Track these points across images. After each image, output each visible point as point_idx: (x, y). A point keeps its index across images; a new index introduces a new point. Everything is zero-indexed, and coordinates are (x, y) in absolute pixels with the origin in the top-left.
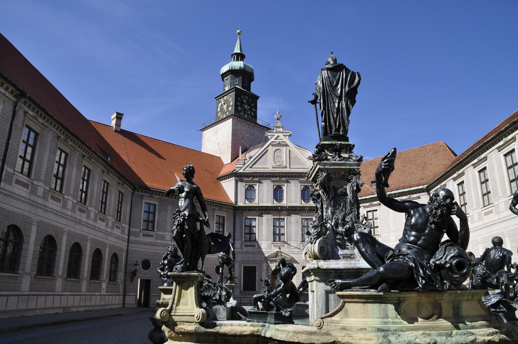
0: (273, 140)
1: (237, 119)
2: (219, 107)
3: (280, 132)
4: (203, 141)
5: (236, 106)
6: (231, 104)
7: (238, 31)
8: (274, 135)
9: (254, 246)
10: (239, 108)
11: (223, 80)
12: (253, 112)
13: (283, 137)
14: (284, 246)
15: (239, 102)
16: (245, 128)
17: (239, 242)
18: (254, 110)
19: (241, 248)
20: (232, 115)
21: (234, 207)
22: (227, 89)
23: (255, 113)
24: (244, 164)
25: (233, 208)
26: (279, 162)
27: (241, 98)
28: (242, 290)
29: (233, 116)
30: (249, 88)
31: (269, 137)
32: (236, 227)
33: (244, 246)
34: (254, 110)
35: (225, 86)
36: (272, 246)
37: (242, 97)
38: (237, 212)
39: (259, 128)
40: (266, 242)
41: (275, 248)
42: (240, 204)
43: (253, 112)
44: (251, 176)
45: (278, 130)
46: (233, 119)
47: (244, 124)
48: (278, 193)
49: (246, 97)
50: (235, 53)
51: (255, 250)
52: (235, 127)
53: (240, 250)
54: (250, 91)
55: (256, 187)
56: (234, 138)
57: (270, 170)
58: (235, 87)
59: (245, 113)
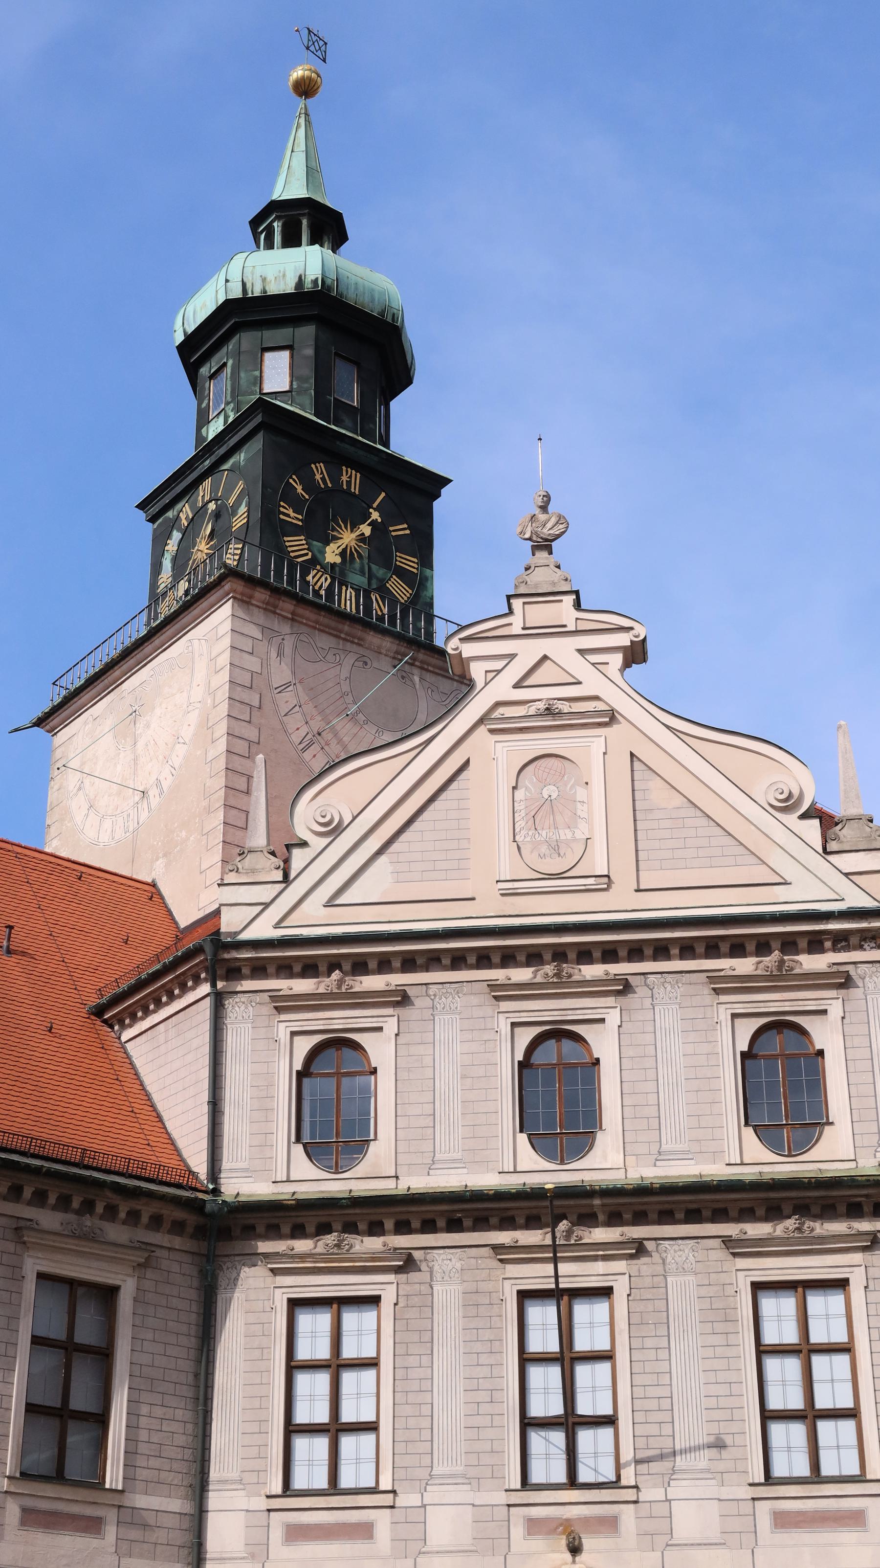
0: (501, 688)
1: (270, 609)
2: (167, 564)
3: (559, 631)
4: (53, 796)
5: (270, 530)
6: (239, 521)
7: (298, 73)
8: (512, 656)
9: (365, 1531)
10: (296, 545)
12: (401, 573)
13: (580, 667)
14: (611, 1524)
15: (297, 504)
17: (240, 1500)
20: (231, 573)
21: (197, 1206)
22: (215, 428)
23: (420, 584)
25: (191, 1219)
26: (556, 849)
27: (309, 484)
29: (239, 586)
31: (477, 671)
33: (277, 1534)
34: (409, 563)
35: (203, 419)
36: (518, 1531)
37: (320, 472)
40: (463, 1494)
41: (538, 1544)
42: (243, 1183)
43: (401, 573)
44: (334, 964)
45: (541, 614)
47: (325, 641)
48: (556, 1090)
49: (351, 480)
50: (275, 207)
52: (253, 664)
57: (489, 909)
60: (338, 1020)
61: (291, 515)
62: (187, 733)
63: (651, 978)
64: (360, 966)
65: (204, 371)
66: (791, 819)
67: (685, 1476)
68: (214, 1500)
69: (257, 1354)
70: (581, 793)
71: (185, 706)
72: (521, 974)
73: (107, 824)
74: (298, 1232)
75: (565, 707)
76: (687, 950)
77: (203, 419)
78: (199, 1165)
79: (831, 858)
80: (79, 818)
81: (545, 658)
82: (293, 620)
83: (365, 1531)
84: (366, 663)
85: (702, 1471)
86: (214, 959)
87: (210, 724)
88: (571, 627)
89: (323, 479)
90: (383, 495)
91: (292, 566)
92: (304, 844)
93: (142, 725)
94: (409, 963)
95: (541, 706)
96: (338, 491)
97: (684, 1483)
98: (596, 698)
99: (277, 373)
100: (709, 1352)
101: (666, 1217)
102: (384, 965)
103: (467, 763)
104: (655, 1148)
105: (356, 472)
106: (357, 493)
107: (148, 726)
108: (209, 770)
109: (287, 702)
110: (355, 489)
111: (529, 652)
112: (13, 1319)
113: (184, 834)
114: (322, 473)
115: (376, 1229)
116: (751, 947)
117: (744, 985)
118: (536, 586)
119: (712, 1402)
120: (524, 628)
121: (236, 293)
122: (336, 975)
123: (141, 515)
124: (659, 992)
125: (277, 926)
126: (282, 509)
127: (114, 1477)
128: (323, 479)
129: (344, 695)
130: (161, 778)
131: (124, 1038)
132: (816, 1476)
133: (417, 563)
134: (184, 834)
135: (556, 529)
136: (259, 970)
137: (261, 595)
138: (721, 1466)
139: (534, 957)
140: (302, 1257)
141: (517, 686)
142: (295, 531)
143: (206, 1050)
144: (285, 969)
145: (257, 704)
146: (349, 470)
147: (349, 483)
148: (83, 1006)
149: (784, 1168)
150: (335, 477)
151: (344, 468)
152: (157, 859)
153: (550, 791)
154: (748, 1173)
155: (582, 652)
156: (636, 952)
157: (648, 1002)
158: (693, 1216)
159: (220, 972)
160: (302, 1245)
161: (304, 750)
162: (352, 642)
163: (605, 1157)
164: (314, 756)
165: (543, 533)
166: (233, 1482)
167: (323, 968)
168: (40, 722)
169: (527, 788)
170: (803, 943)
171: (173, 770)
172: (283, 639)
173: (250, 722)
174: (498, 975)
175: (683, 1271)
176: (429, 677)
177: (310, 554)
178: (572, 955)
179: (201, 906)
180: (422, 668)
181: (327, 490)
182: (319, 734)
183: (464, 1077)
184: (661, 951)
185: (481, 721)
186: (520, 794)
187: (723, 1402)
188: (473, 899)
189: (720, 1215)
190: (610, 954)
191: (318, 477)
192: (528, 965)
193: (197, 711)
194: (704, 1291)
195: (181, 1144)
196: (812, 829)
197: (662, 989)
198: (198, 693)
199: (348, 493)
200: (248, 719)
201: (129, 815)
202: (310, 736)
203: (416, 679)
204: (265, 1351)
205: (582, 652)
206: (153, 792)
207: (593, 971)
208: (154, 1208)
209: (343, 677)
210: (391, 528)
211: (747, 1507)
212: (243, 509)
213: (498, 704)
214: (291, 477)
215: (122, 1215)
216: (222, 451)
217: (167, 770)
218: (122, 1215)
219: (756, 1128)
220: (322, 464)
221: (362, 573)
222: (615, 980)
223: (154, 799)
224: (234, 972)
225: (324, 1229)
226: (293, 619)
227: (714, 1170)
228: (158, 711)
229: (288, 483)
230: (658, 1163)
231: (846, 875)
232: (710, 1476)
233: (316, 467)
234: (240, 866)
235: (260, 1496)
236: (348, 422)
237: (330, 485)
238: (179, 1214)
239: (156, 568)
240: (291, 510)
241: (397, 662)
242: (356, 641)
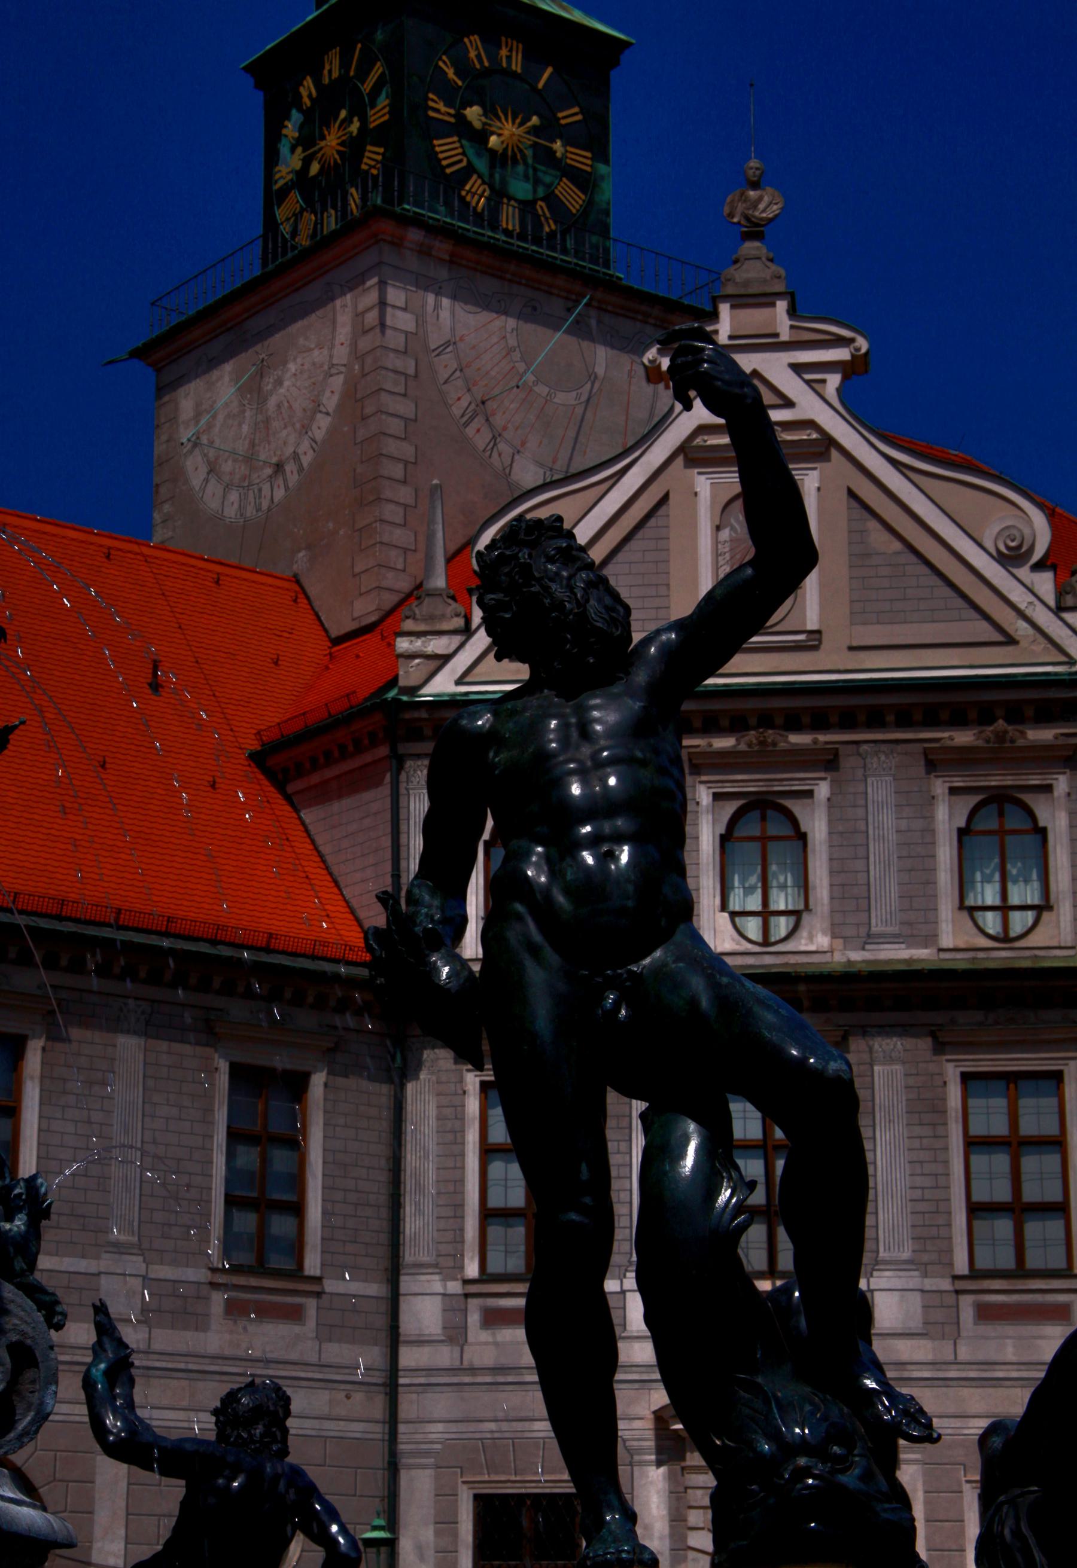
17: (436, 1284)
19: (455, 1334)
27: (463, 68)
32: (411, 1160)
33: (474, 1318)
37: (474, 48)
53: (445, 1356)
62: (331, 402)
63: (864, 747)
67: (888, 1267)
68: (407, 1284)
69: (449, 1137)
71: (326, 367)
73: (234, 496)
76: (904, 720)
80: (196, 482)
82: (451, 262)
84: (535, 309)
85: (906, 1262)
87: (359, 396)
88: (785, 337)
89: (479, 56)
90: (550, 70)
93: (271, 380)
96: (496, 71)
97: (887, 1273)
100: (916, 1143)
103: (665, 499)
104: (863, 931)
105: (518, 42)
106: (519, 71)
107: (279, 382)
108: (359, 452)
109: (446, 366)
110: (517, 66)
112: (209, 1110)
113: (331, 525)
114: (477, 48)
118: (747, 283)
119: (918, 1194)
124: (873, 762)
125: (459, 682)
126: (431, 104)
127: (312, 1264)
128: (479, 56)
129: (510, 351)
130: (300, 451)
132: (1021, 1271)
133: (592, 159)
134: (331, 525)
135: (769, 211)
138: (925, 1258)
145: (411, 371)
146: (509, 40)
147: (509, 58)
148: (240, 751)
149: (1002, 957)
150: (494, 58)
151: (503, 39)
152: (299, 551)
157: (860, 773)
161: (466, 424)
162: (519, 283)
163: (811, 938)
164: (478, 431)
165: (754, 217)
166: (429, 1266)
168: (137, 354)
169: (733, 529)
171: (314, 445)
172: (440, 288)
173: (405, 395)
175: (890, 1060)
177: (465, 160)
179: (356, 615)
180: (599, 309)
181: (486, 73)
182: (483, 403)
186: (725, 534)
187: (928, 1194)
191: (472, 54)
193: (341, 377)
194: (911, 1081)
197: (875, 759)
198: (341, 353)
200: (403, 391)
201: (260, 490)
202: (473, 406)
203: (593, 322)
204: (458, 1135)
206: (290, 467)
209: (509, 329)
210: (560, 115)
211: (951, 1299)
212: (383, 101)
214: (440, 59)
215: (310, 1000)
217: (305, 445)
218: (310, 1000)
220: (476, 37)
221: (526, 178)
223: (292, 476)
226: (453, 262)
227: (922, 954)
228: (292, 367)
229: (437, 66)
230: (867, 947)
232: (914, 1267)
233: (471, 42)
234: (417, 612)
235: (457, 1280)
237: (486, 64)
239: (272, 157)
240: (442, 104)
241: (570, 304)
242: (523, 281)
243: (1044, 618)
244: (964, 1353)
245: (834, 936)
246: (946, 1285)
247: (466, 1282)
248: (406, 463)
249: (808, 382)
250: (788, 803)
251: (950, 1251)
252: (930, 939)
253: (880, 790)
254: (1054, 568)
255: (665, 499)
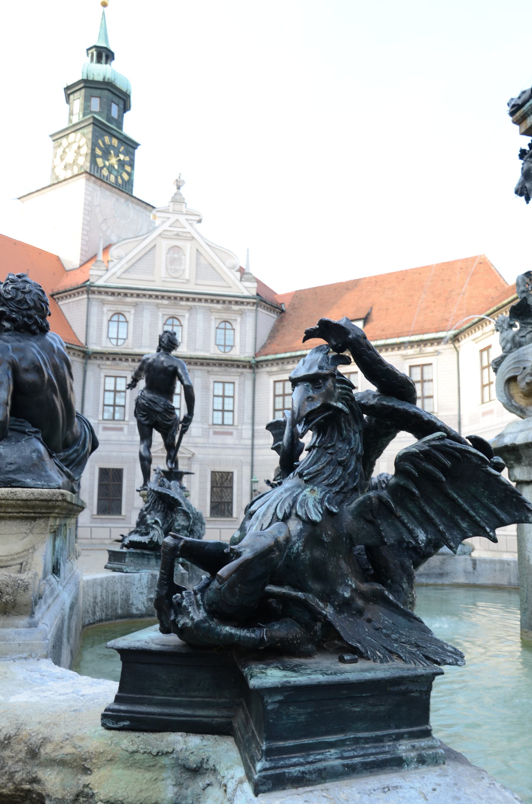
0: (166, 226)
1: (95, 183)
5: (94, 156)
8: (169, 218)
9: (121, 429)
10: (100, 161)
11: (68, 101)
13: (186, 224)
16: (109, 201)
18: (128, 168)
24: (107, 270)
25: (82, 354)
26: (176, 271)
28: (95, 512)
29: (88, 175)
30: (119, 123)
32: (87, 392)
37: (107, 139)
38: (89, 362)
39: (138, 204)
44: (119, 294)
46: (88, 180)
47: (108, 193)
49: (115, 142)
51: (123, 438)
54: (121, 128)
55: (130, 317)
56: (88, 218)
58: (94, 118)
59: (110, 173)
60: (120, 308)
61: (98, 152)
64: (126, 295)
65: (71, 97)
66: (233, 271)
70: (183, 257)
72: (165, 302)
74: (108, 359)
75: (181, 234)
77: (71, 114)
78: (83, 341)
79: (243, 283)
81: (177, 220)
83: (121, 429)
86: (87, 288)
91: (98, 167)
92: (112, 261)
94: (138, 296)
95: (176, 233)
98: (189, 233)
99: (95, 104)
101: (196, 364)
102: (132, 295)
103: (155, 246)
110: (116, 145)
111: (173, 218)
115: (127, 360)
116: (221, 302)
117: (219, 311)
120: (173, 211)
121: (85, 78)
122: (120, 297)
123: (50, 139)
131: (60, 303)
136: (100, 293)
137: (93, 179)
139: (169, 298)
140: (108, 365)
141: (170, 226)
142: (99, 157)
143: (85, 312)
144: (107, 293)
149: (224, 356)
150: (111, 142)
153: (176, 256)
154: (215, 356)
155: (187, 220)
156: (194, 300)
158: (202, 364)
159: (90, 292)
160: (108, 363)
167: (116, 294)
170: (233, 303)
174: (159, 301)
176: (134, 205)
178: (178, 299)
181: (109, 145)
183: (150, 326)
184: (200, 300)
185: (160, 235)
186: (168, 255)
188: (154, 281)
189: (208, 365)
190: (188, 299)
192: (167, 300)
195: (77, 334)
196: (238, 274)
199: (114, 146)
203: (130, 205)
205: (187, 220)
207: (183, 303)
208: (74, 351)
213: (165, 230)
216: (78, 127)
219: (218, 345)
222: (188, 306)
224: (93, 292)
225: (114, 359)
226: (101, 186)
227: (207, 355)
231: (245, 287)
236: (115, 123)
238: (79, 353)
243: (238, 283)
244: (210, 441)
245: (188, 348)
246: (207, 426)
247: (99, 420)
248: (87, 231)
249: (190, 224)
250: (179, 318)
251: (208, 419)
252: (208, 351)
253: (200, 317)
254: (240, 272)
255: (155, 246)
